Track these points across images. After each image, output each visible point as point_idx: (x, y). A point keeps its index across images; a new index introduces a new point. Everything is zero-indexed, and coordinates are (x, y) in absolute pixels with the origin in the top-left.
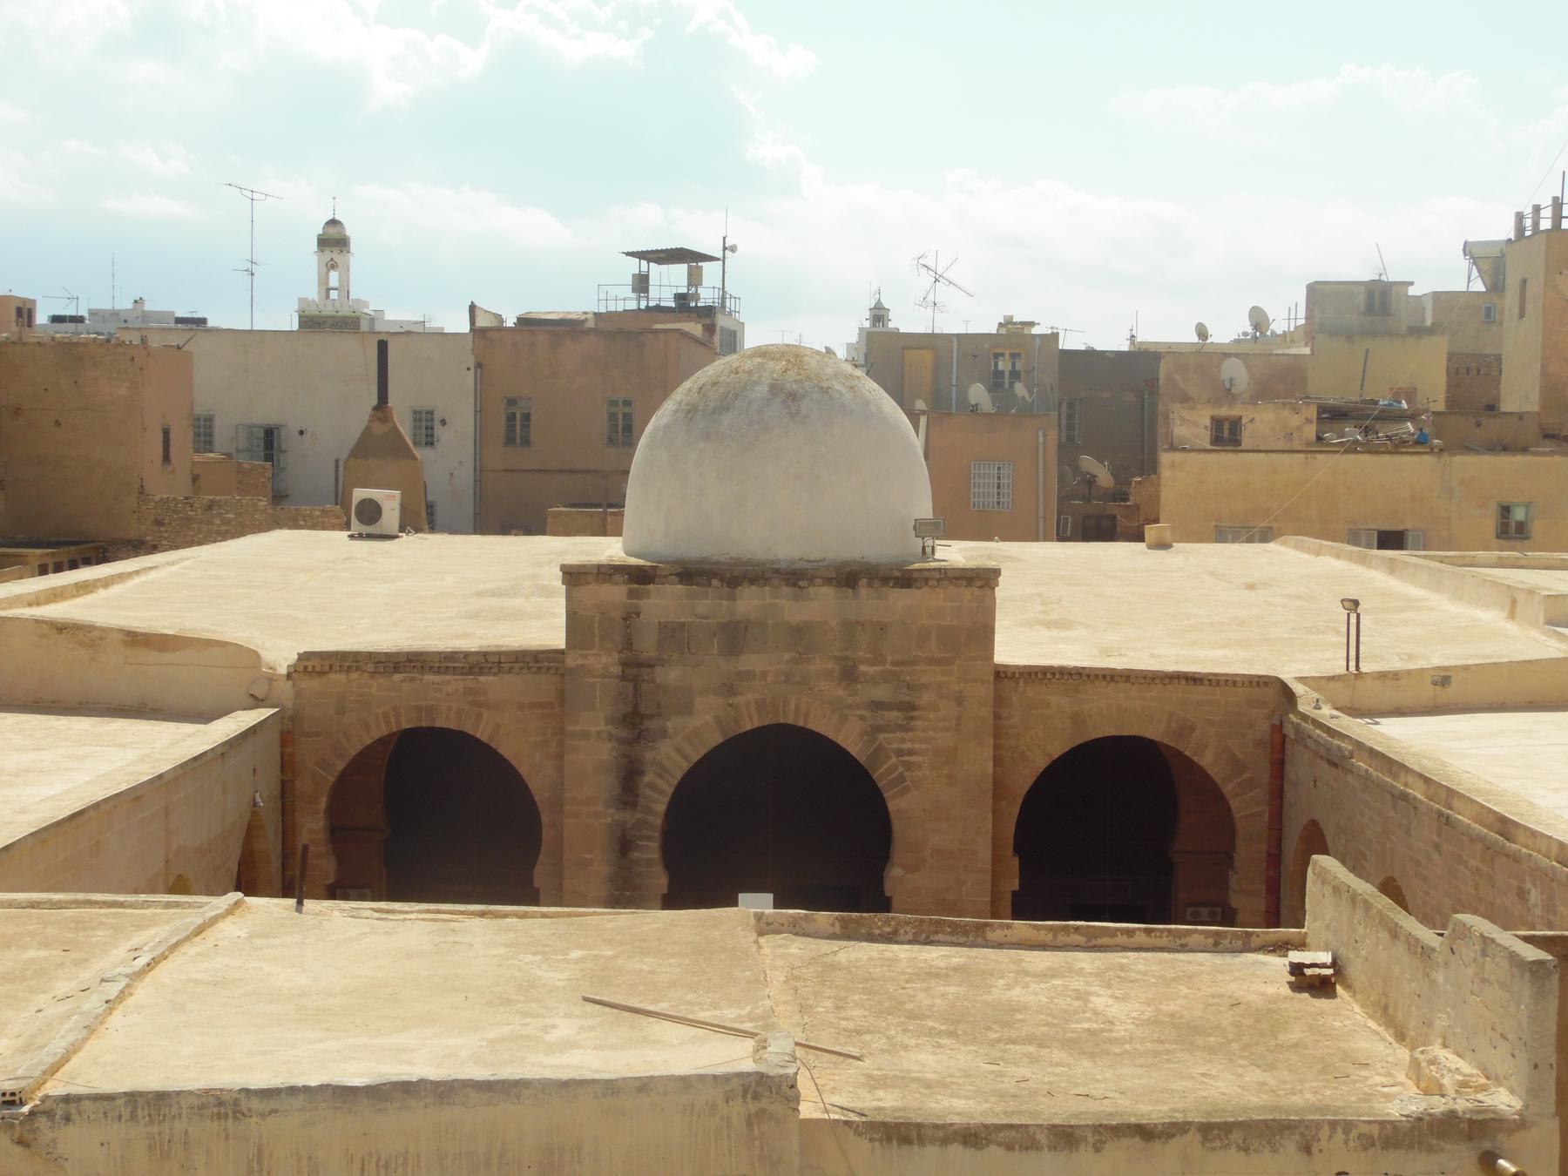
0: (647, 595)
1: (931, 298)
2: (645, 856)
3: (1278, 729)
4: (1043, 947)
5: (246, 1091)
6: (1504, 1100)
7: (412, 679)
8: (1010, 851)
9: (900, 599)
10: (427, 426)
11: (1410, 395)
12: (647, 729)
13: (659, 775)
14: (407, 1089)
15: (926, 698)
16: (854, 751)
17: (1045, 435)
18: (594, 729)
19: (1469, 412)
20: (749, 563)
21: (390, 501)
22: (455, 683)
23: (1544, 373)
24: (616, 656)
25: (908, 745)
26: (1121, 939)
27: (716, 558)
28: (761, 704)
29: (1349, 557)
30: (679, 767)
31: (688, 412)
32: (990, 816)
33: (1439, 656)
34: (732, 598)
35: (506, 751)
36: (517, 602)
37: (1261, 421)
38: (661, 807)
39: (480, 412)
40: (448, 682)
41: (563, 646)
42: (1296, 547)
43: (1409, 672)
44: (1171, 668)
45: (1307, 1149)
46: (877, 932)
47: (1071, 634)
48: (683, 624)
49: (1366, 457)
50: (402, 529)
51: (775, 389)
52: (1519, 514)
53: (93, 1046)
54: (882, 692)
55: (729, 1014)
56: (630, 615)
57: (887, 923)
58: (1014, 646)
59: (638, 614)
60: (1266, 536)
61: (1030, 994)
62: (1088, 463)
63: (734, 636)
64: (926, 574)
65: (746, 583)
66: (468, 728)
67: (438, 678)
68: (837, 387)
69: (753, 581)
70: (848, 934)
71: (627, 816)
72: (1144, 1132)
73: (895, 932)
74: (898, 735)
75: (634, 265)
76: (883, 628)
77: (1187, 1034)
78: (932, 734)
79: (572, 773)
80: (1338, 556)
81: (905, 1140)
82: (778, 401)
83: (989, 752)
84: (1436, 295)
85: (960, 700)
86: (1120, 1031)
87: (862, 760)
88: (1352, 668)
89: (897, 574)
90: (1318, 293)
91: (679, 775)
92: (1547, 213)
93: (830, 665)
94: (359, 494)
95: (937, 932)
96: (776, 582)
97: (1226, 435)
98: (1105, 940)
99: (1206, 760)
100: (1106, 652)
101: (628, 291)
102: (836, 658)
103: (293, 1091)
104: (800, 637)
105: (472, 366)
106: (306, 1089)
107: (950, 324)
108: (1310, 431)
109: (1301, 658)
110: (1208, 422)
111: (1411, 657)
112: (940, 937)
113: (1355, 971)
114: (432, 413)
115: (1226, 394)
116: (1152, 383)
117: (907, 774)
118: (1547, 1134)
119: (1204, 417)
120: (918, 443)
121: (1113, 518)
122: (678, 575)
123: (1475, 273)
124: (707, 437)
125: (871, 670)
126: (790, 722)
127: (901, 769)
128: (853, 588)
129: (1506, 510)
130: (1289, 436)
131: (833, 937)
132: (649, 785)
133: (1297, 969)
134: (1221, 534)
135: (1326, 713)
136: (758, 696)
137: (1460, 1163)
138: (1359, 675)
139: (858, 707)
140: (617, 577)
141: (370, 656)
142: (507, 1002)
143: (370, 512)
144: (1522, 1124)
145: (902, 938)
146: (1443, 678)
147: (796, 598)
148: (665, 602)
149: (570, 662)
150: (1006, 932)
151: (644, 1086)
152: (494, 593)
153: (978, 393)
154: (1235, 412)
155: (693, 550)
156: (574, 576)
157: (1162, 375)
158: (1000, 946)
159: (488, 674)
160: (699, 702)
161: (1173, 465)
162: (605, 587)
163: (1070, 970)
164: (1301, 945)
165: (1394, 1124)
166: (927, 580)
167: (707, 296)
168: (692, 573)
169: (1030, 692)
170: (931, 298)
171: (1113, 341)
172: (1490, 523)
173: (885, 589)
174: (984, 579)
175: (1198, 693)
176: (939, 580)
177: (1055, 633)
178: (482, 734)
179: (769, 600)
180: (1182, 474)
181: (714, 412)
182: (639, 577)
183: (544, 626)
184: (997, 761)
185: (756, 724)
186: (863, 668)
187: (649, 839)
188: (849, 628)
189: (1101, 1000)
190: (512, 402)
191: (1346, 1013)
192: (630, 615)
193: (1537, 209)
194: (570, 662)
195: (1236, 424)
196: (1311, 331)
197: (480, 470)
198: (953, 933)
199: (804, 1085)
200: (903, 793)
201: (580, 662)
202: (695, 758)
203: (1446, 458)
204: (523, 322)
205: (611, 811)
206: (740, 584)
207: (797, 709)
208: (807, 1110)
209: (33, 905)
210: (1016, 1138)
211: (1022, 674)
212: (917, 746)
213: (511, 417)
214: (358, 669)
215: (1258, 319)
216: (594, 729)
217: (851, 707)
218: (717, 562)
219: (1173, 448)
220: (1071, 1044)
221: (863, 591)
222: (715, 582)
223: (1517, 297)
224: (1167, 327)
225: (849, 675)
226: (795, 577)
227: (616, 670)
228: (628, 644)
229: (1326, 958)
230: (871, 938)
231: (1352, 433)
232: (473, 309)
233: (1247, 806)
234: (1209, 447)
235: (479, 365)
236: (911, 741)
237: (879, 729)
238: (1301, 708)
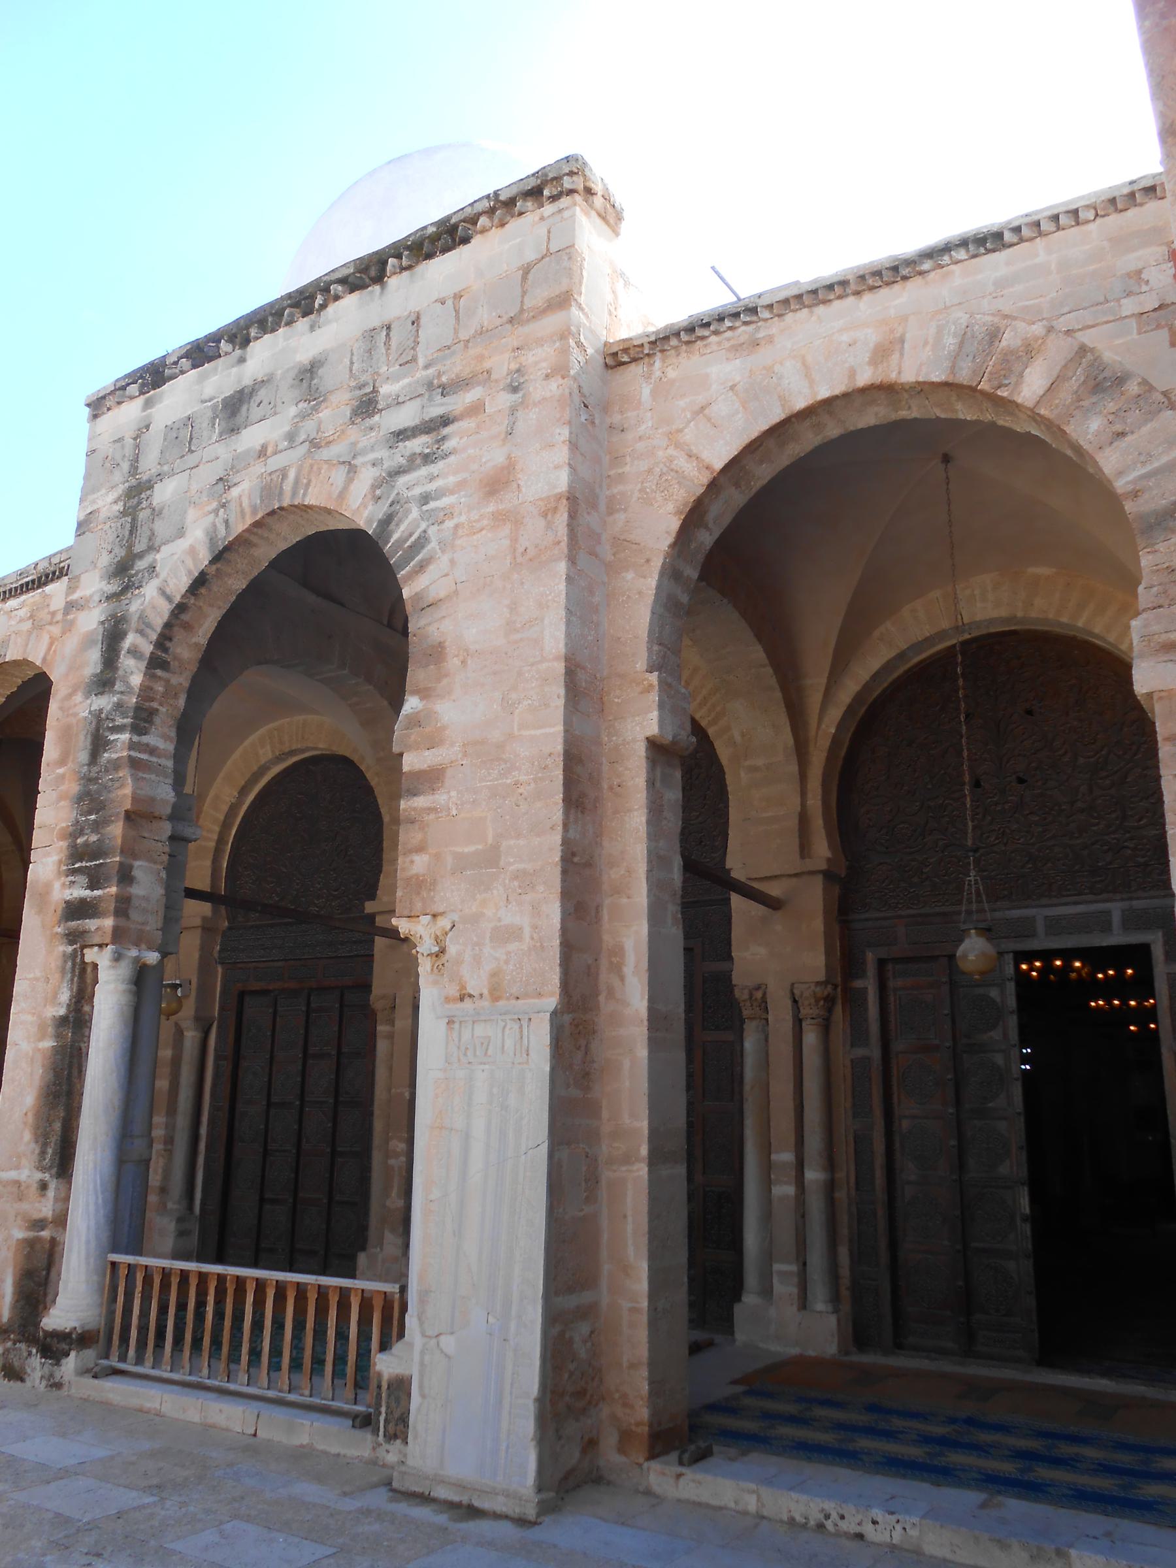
54: (406, 416)
71: (104, 702)
74: (424, 471)
78: (471, 451)
117: (432, 531)
127: (423, 525)
139: (372, 449)
140: (133, 389)
159: (52, 580)
166: (473, 220)
175: (996, 264)
200: (422, 567)
207: (297, 481)
228: (134, 469)
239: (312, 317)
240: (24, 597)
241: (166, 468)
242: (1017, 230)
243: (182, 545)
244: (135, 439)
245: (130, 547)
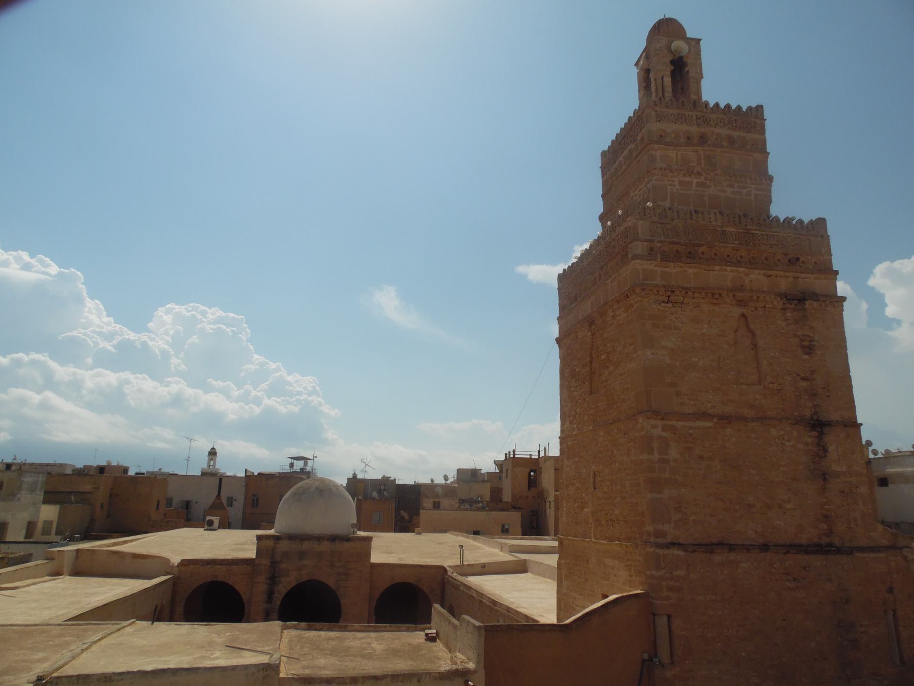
3: (443, 579)
4: (362, 631)
5: (114, 674)
6: (471, 665)
9: (347, 545)
10: (231, 501)
14: (163, 671)
16: (332, 587)
19: (496, 501)
21: (216, 520)
33: (483, 560)
35: (237, 587)
36: (246, 546)
37: (445, 502)
38: (279, 603)
39: (245, 498)
45: (419, 681)
50: (219, 528)
51: (317, 489)
52: (506, 527)
53: (74, 662)
55: (266, 649)
58: (376, 557)
60: (445, 532)
61: (356, 644)
63: (302, 555)
70: (309, 629)
72: (376, 678)
75: (290, 461)
77: (395, 653)
79: (254, 593)
81: (309, 683)
86: (377, 652)
90: (459, 471)
94: (208, 518)
97: (436, 506)
103: (129, 673)
106: (133, 672)
107: (368, 477)
108: (457, 505)
109: (449, 561)
113: (441, 635)
115: (437, 496)
118: (482, 674)
119: (431, 501)
120: (354, 505)
129: (503, 526)
133: (427, 635)
137: (458, 683)
141: (201, 560)
142: (203, 647)
143: (210, 523)
144: (474, 672)
146: (483, 566)
148: (284, 545)
149: (257, 562)
151: (234, 668)
153: (375, 494)
156: (259, 538)
163: (368, 637)
164: (430, 629)
165: (442, 673)
167: (308, 469)
168: (292, 537)
171: (410, 482)
174: (369, 539)
178: (230, 583)
180: (425, 515)
182: (277, 538)
183: (251, 553)
189: (375, 645)
191: (439, 646)
194: (257, 562)
195: (439, 503)
199: (282, 668)
204: (260, 474)
208: (282, 675)
209: (72, 625)
210: (340, 680)
220: (363, 656)
224: (424, 480)
226: (319, 539)
227: (269, 564)
229: (434, 631)
230: (315, 630)
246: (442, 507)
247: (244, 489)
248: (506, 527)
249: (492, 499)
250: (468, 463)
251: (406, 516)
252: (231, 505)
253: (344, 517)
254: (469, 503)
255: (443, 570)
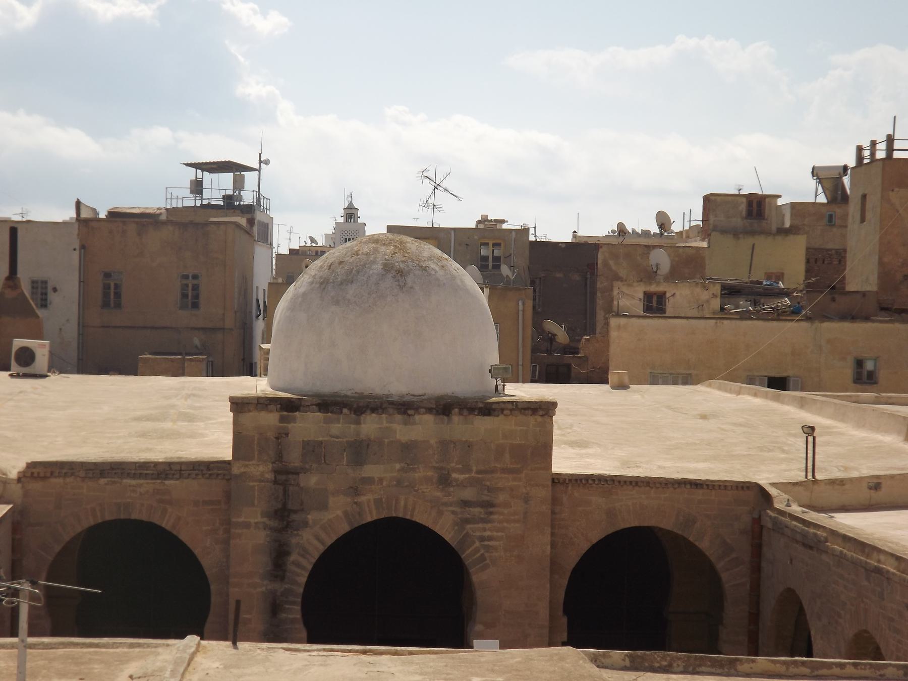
0: (294, 420)
1: (431, 201)
2: (291, 616)
7: (114, 483)
8: (560, 612)
9: (483, 424)
11: (780, 277)
12: (293, 521)
13: (303, 556)
15: (502, 497)
17: (524, 304)
18: (253, 521)
19: (825, 290)
20: (370, 396)
22: (147, 485)
23: (881, 263)
24: (270, 466)
25: (488, 533)
26: (836, 671)
27: (344, 392)
28: (378, 502)
29: (766, 396)
30: (316, 549)
31: (321, 283)
32: (548, 586)
33: (866, 469)
34: (358, 423)
35: (184, 537)
36: (168, 425)
37: (680, 296)
38: (303, 579)
39: (83, 282)
40: (140, 486)
41: (231, 458)
42: (720, 389)
43: (851, 480)
44: (678, 476)
46: (657, 665)
47: (590, 451)
48: (321, 442)
49: (760, 323)
51: (388, 267)
52: (869, 366)
54: (468, 494)
56: (282, 435)
57: (664, 658)
58: (565, 461)
59: (287, 435)
60: (687, 380)
62: (550, 325)
63: (359, 451)
64: (503, 406)
65: (369, 411)
66: (156, 520)
67: (134, 482)
68: (433, 266)
69: (374, 410)
70: (635, 666)
71: (278, 587)
73: (670, 665)
74: (480, 525)
75: (192, 174)
76: (469, 445)
79: (238, 555)
80: (755, 395)
82: (390, 276)
83: (547, 539)
84: (793, 205)
85: (526, 499)
87: (454, 544)
88: (810, 476)
89: (481, 405)
90: (711, 202)
91: (317, 555)
92: (881, 147)
93: (430, 473)
94: (19, 343)
95: (700, 666)
96: (391, 410)
97: (655, 305)
98: (824, 672)
99: (704, 545)
100: (626, 464)
101: (187, 193)
102: (435, 468)
104: (408, 452)
105: (77, 247)
108: (716, 303)
109: (773, 468)
110: (641, 296)
111: (846, 469)
112: (703, 669)
114: (45, 282)
115: (650, 275)
116: (593, 266)
117: (487, 555)
119: (639, 291)
121: (569, 366)
122: (318, 405)
123: (820, 190)
124: (337, 303)
125: (462, 477)
126: (401, 515)
127: (482, 551)
128: (448, 415)
129: (859, 363)
130: (700, 306)
131: (625, 669)
132: (293, 563)
134: (654, 380)
135: (795, 509)
136: (376, 496)
138: (815, 482)
139: (451, 505)
140: (272, 407)
141: (82, 465)
143: (26, 357)
145: (675, 669)
146: (876, 484)
147: (405, 423)
148: (308, 426)
149: (236, 470)
150: (752, 665)
152: (149, 418)
154: (661, 289)
155: (329, 386)
156: (239, 405)
157: (600, 262)
158: (748, 675)
159: (172, 479)
160: (332, 500)
161: (619, 327)
162: (263, 414)
166: (502, 410)
167: (248, 197)
168: (329, 404)
169: (576, 494)
170: (431, 201)
171: (564, 236)
172: (849, 372)
173: (471, 416)
174: (546, 409)
175: (699, 494)
176: (511, 410)
177: (577, 450)
178: (166, 524)
179: (385, 424)
180: (627, 332)
181: (342, 283)
183: (216, 441)
184: (553, 545)
185: (375, 518)
186: (454, 475)
187: (294, 603)
188: (445, 445)
190: (107, 275)
192: (282, 435)
193: (874, 144)
194: (236, 470)
195: (661, 297)
196: (707, 229)
197: (83, 325)
198: (712, 666)
201: (242, 470)
202: (329, 542)
203: (817, 324)
204: (113, 215)
205: (265, 582)
206: (362, 413)
211: (570, 480)
212: (495, 534)
213: (107, 287)
214: (72, 474)
215: (663, 221)
216: (253, 521)
217: (445, 504)
218: (346, 396)
219: (618, 315)
221: (456, 418)
222: (345, 411)
223: (859, 207)
224: (597, 226)
225: (444, 481)
226: (405, 407)
227: (270, 476)
228: (280, 457)
231: (744, 304)
232: (78, 204)
233: (734, 579)
234: (642, 313)
235: (83, 247)
236: (490, 530)
237: (467, 521)
238: (779, 505)
239: (405, 416)
240: (142, 481)
241: (307, 467)
242: (707, 485)
243: (327, 516)
244: (277, 438)
245: (285, 505)
246: (669, 311)
247: (76, 256)
248: (869, 366)
249: (811, 288)
250: (738, 177)
251: (561, 335)
252: (44, 304)
253: (462, 341)
254: (747, 296)
255: (761, 495)
